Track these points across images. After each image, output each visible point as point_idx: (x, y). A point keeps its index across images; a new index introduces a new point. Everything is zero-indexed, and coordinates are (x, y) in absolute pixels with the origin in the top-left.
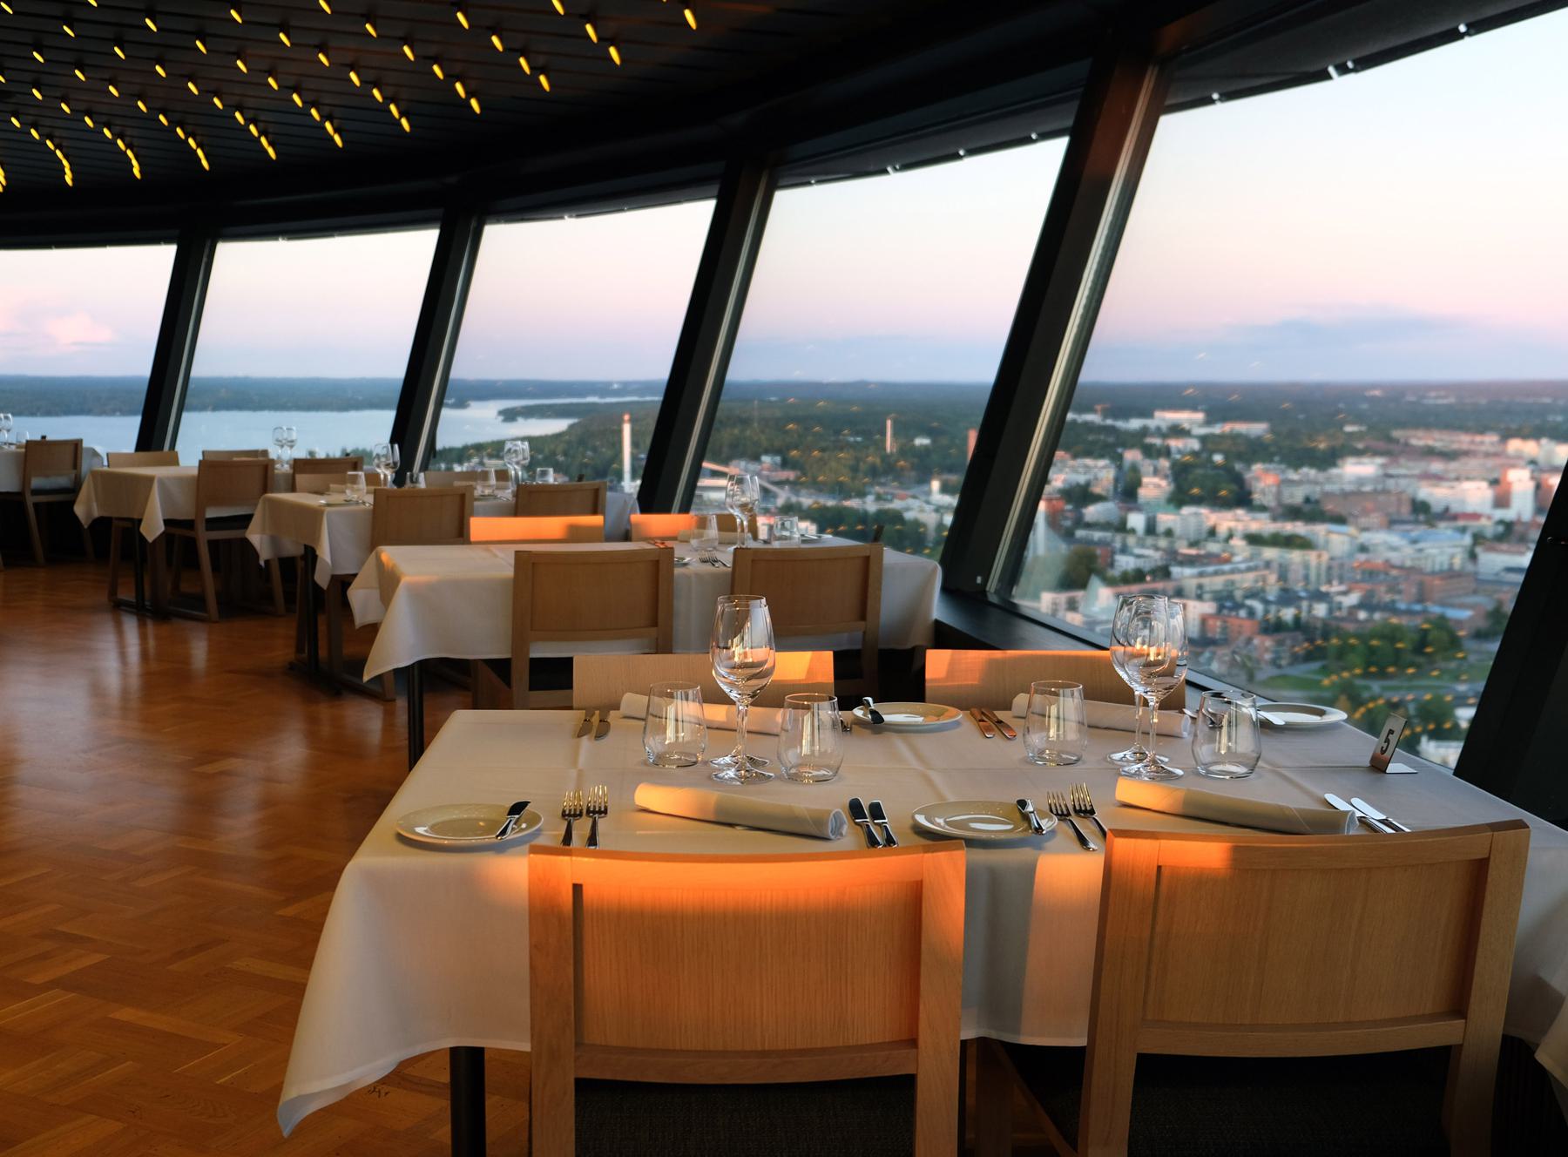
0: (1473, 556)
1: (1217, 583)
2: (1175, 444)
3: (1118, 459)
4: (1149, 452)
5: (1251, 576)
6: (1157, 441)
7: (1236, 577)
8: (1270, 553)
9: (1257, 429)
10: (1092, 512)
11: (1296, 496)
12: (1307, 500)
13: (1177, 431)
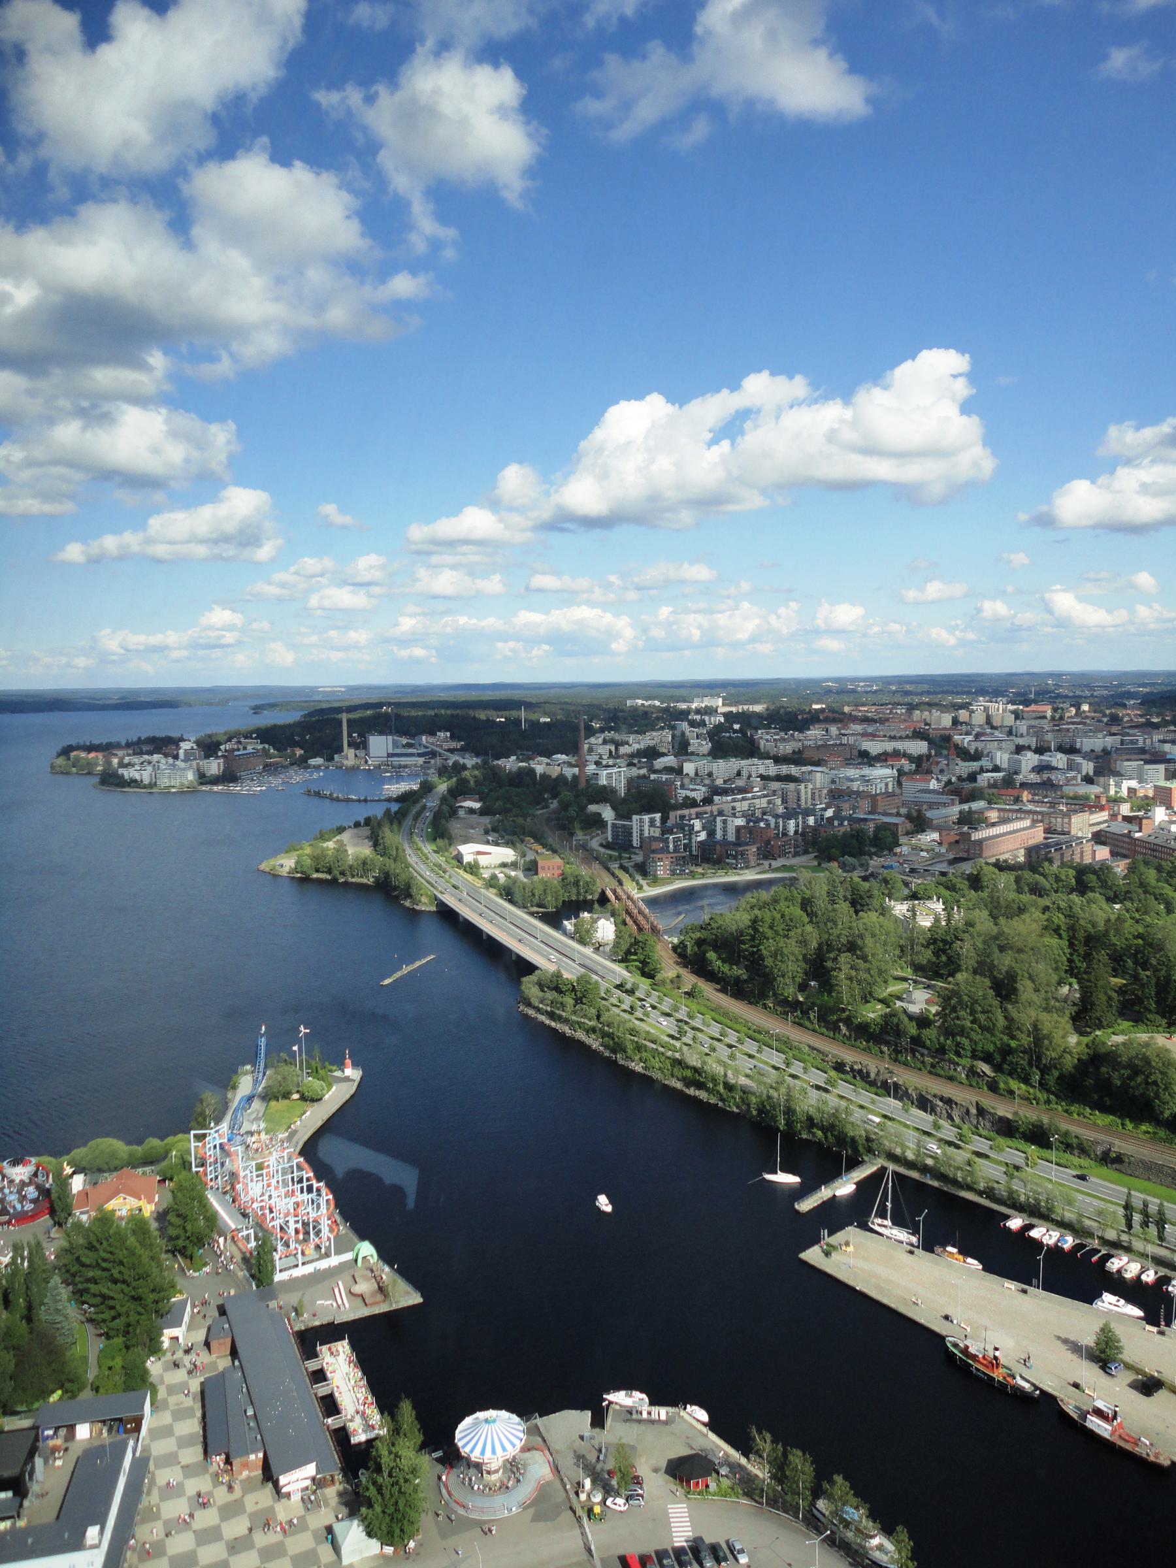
0: (899, 784)
1: (745, 806)
2: (707, 718)
3: (673, 728)
4: (693, 724)
5: (765, 800)
6: (698, 717)
7: (757, 801)
8: (775, 785)
9: (758, 708)
10: (660, 763)
11: (787, 748)
12: (794, 752)
13: (710, 711)
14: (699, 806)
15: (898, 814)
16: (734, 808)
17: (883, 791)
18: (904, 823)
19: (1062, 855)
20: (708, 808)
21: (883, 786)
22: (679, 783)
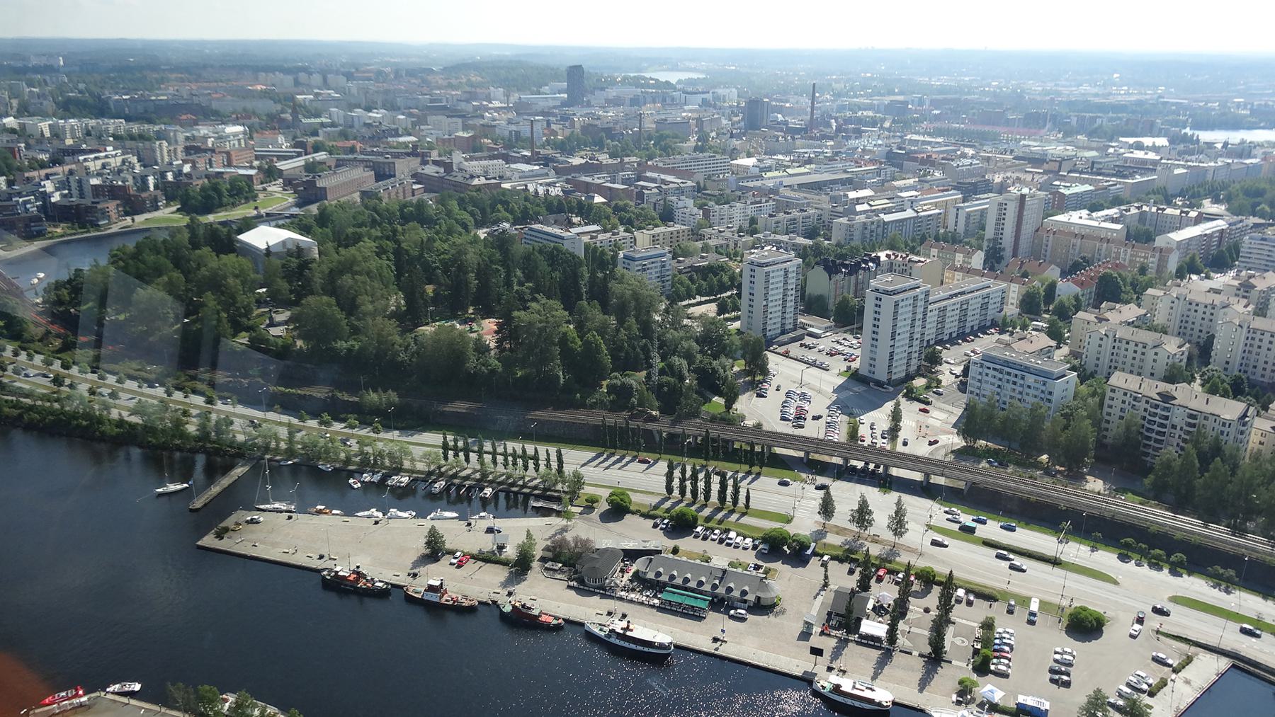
14: (50, 167)
15: (252, 167)
16: (87, 168)
17: (237, 146)
18: (257, 174)
19: (389, 194)
20: (58, 169)
21: (236, 143)
22: (23, 145)
